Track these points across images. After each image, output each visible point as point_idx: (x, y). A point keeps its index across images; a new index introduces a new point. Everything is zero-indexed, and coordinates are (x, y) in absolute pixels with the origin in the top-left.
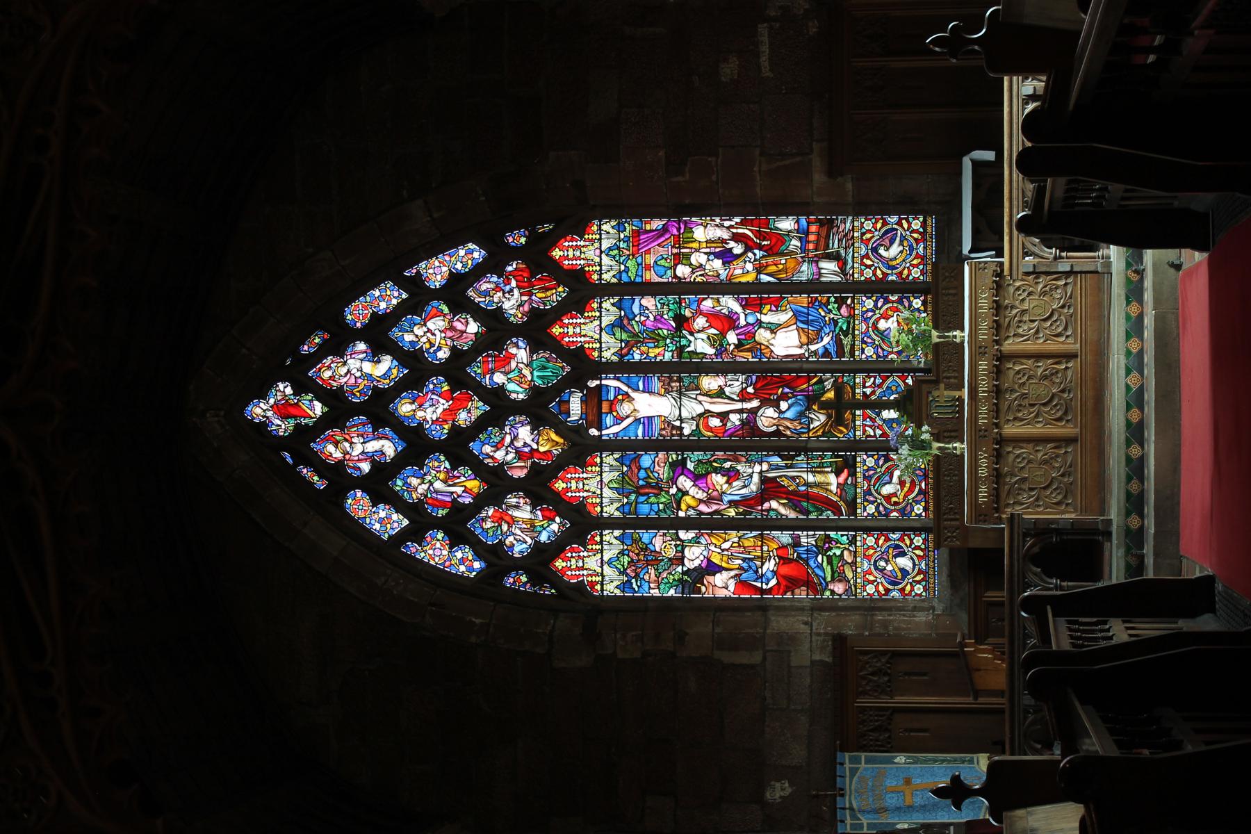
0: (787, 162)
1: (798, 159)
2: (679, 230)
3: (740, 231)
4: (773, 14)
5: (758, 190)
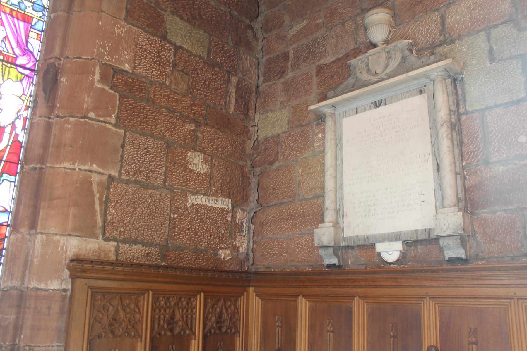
0: (97, 207)
1: (99, 221)
2: (23, 67)
3: (6, 136)
4: (239, 215)
5: (67, 165)
